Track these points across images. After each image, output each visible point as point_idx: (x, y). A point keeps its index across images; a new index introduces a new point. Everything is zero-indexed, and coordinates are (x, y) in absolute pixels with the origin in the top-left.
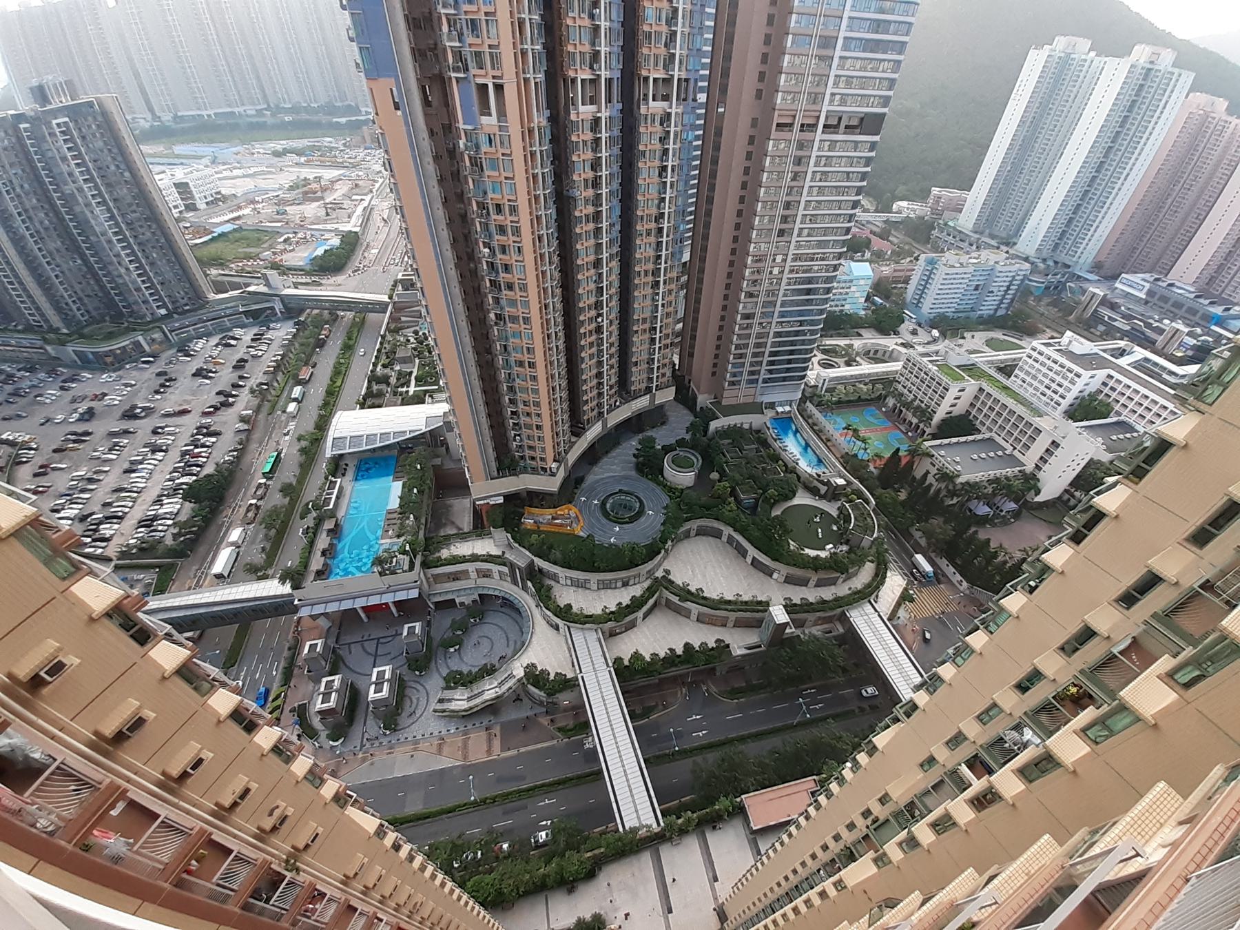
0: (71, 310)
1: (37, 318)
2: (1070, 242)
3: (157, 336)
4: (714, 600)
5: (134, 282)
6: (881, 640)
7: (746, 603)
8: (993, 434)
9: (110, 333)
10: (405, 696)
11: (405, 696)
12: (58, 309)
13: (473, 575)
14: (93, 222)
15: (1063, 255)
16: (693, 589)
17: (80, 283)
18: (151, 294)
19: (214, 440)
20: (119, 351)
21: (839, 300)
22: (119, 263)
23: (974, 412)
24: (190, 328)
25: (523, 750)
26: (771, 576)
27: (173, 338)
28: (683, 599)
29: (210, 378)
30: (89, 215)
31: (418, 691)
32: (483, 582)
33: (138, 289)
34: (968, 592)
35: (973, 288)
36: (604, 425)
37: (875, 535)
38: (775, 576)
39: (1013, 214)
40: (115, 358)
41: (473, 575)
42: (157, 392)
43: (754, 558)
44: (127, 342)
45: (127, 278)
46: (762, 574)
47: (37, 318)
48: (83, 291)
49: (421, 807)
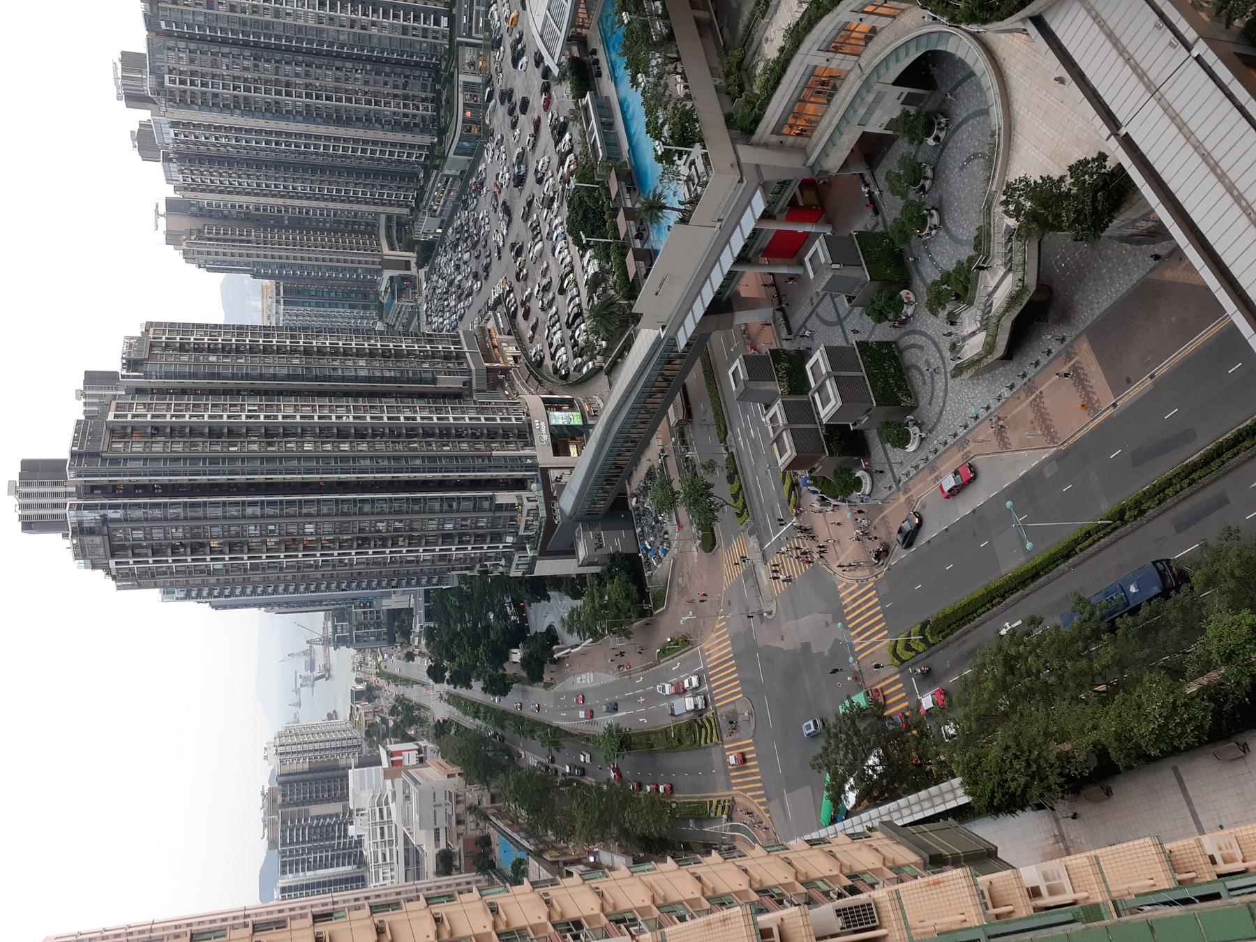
0: (414, 116)
1: (416, 153)
3: (467, 55)
5: (393, 27)
9: (448, 101)
10: (908, 368)
11: (908, 368)
12: (406, 128)
13: (839, 62)
14: (301, 22)
17: (386, 83)
18: (416, 18)
19: (567, 137)
20: (468, 114)
22: (363, 28)
24: (475, 7)
25: (1162, 369)
27: (478, 38)
29: (523, 50)
30: (289, 21)
31: (921, 348)
32: (874, 53)
33: (405, 30)
40: (475, 123)
41: (839, 62)
42: (514, 126)
44: (461, 96)
45: (386, 33)
47: (416, 153)
48: (396, 87)
49: (1022, 559)
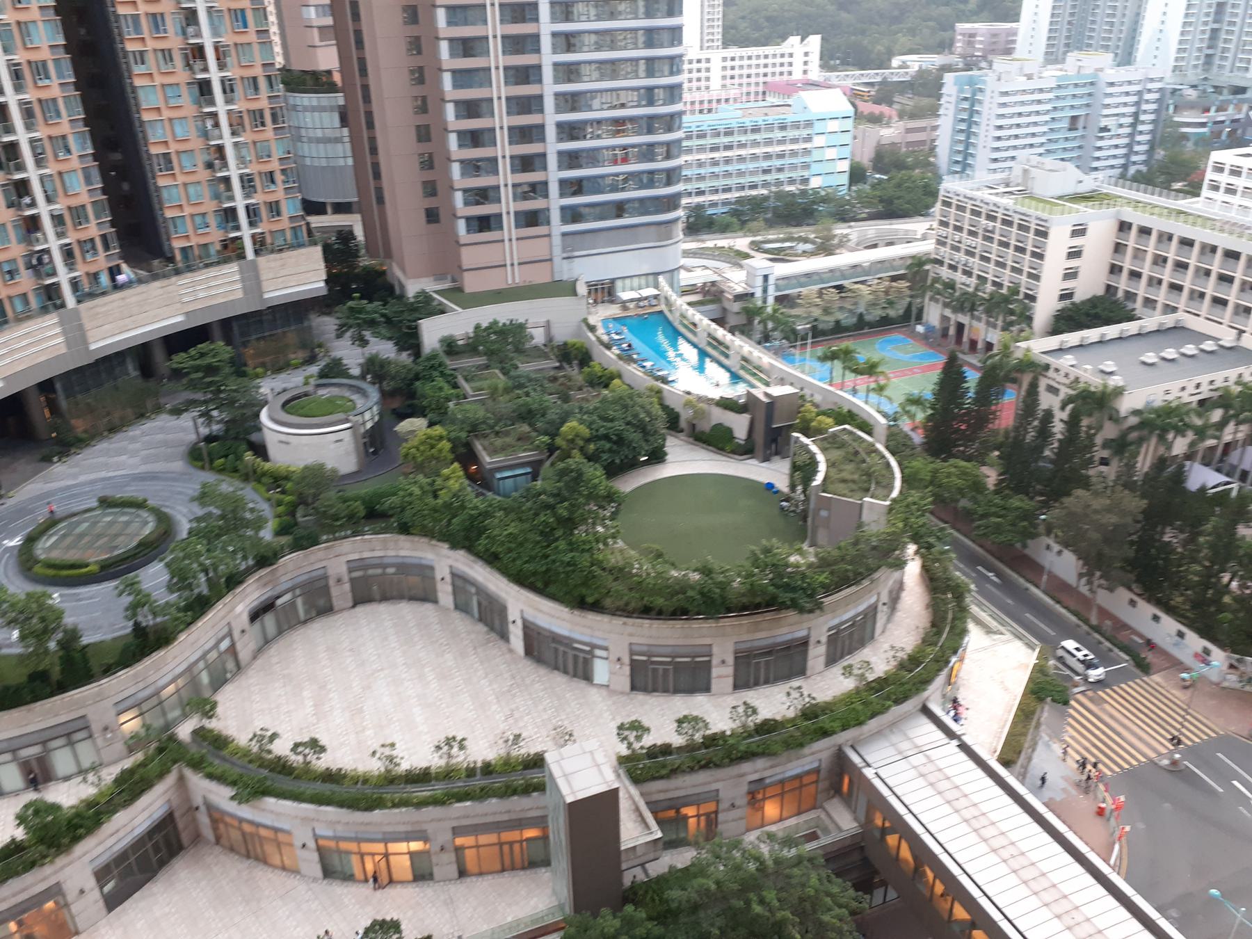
2: (1232, 46)
4: (366, 780)
6: (976, 823)
7: (487, 769)
8: (1180, 315)
15: (1226, 72)
16: (281, 748)
21: (793, 167)
23: (1123, 284)
26: (587, 676)
28: (252, 790)
34: (1232, 680)
35: (1065, 124)
36: (76, 334)
37: (895, 494)
38: (601, 670)
39: (1112, 24)
43: (454, 575)
46: (559, 679)
